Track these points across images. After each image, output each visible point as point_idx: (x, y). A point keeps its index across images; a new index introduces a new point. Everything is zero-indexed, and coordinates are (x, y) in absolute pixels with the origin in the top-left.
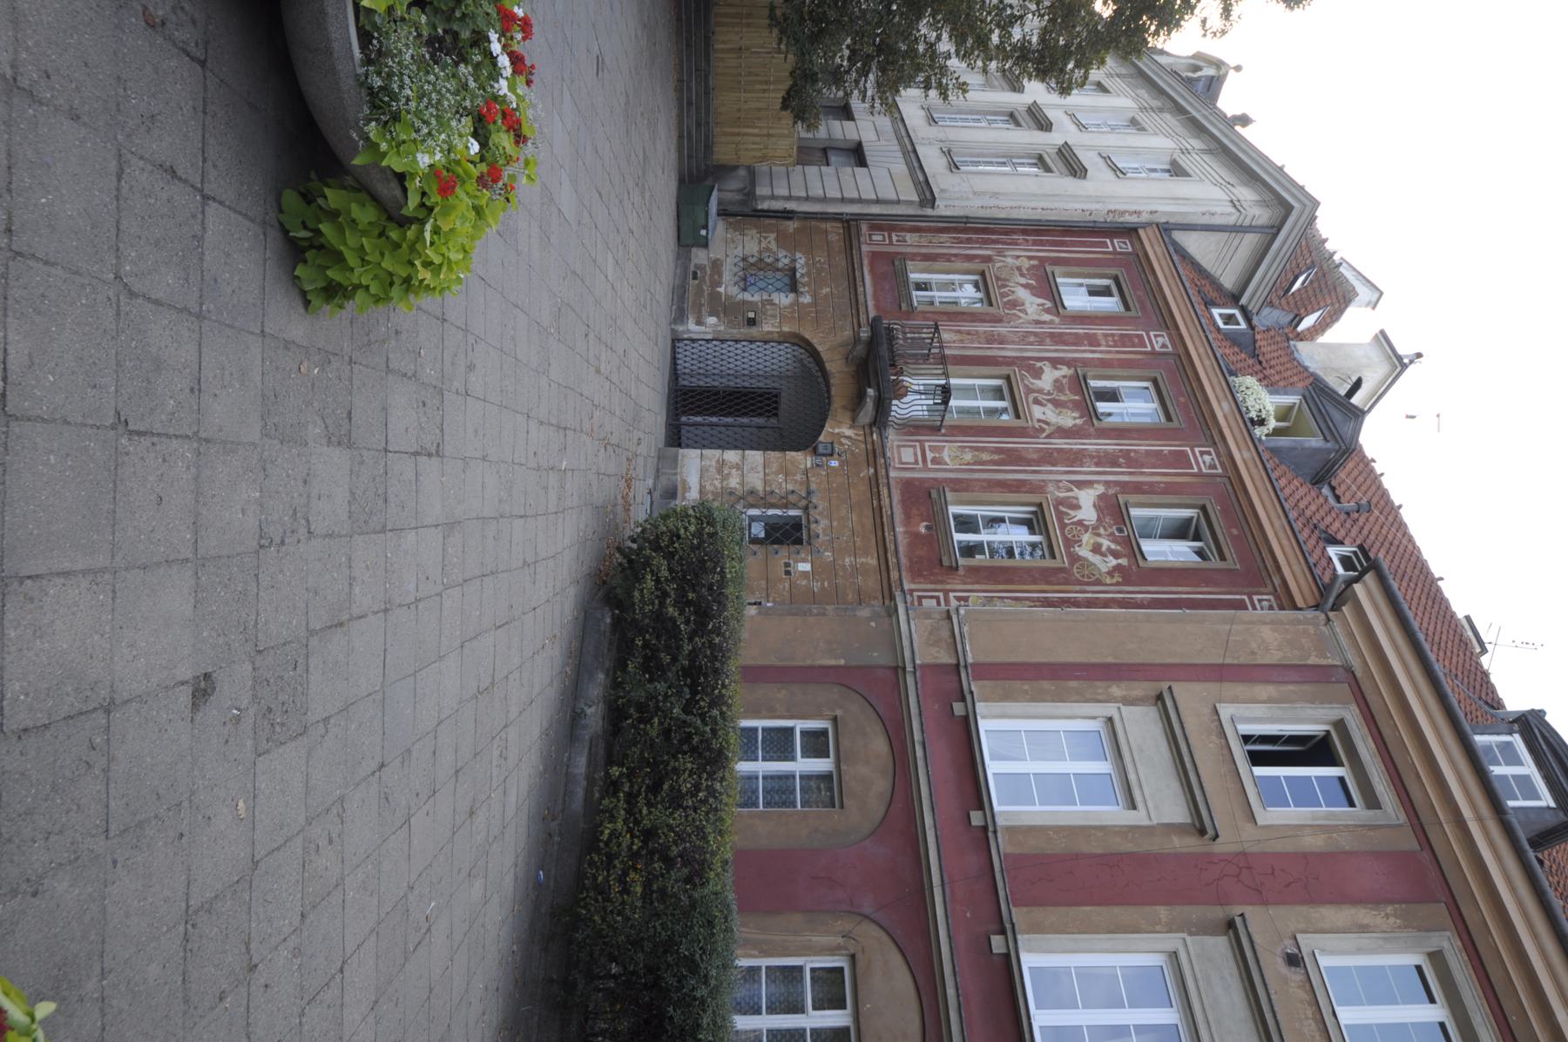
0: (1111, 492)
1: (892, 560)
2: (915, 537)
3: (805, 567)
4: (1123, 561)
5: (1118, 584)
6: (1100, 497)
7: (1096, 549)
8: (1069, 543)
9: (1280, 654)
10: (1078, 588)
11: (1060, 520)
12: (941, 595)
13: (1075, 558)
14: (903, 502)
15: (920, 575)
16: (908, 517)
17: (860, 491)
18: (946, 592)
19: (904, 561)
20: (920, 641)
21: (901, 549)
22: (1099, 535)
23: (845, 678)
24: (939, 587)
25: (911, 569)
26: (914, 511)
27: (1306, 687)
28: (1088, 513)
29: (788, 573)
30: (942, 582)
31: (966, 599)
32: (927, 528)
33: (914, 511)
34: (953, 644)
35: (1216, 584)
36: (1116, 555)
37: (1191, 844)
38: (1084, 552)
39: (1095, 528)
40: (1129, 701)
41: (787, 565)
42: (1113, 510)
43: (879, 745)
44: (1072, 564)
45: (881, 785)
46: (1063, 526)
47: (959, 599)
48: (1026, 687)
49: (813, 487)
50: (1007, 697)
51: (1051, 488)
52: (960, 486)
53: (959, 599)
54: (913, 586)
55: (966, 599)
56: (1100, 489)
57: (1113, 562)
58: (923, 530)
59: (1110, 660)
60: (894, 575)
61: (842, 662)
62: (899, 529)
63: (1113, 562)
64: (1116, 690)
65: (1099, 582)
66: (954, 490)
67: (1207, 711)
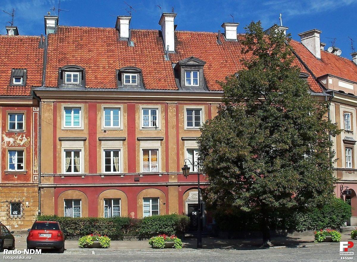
0: (5, 133)
1: (26, 185)
2: (18, 179)
3: (27, 203)
4: (24, 135)
5: (30, 138)
6: (6, 136)
7: (21, 140)
8: (19, 146)
9: (51, 113)
10: (31, 147)
11: (13, 146)
12: (34, 176)
13: (23, 145)
14: (9, 181)
15: (28, 179)
16: (13, 180)
17: (6, 190)
18: (33, 175)
19: (25, 182)
20: (49, 182)
21: (21, 183)
22: (17, 139)
23: (57, 197)
24: (32, 176)
25: (27, 181)
26: (11, 178)
27: (58, 111)
28: (11, 140)
29: (29, 207)
30: (30, 174)
31: (35, 171)
32: (16, 176)
33: (11, 178)
34: (50, 176)
35: (30, 117)
36: (22, 136)
37: (87, 141)
38: (22, 143)
39: (15, 139)
40: (61, 145)
41: (27, 207)
42: (9, 135)
43: (70, 192)
44: (25, 147)
45: (77, 192)
46: (14, 146)
47: (35, 172)
48: (58, 164)
49: (5, 201)
50: (60, 168)
51: (4, 147)
52: (4, 167)
53: (35, 172)
54: (32, 181)
55: (35, 171)
56: (4, 136)
57: (24, 138)
58: (16, 177)
59: (52, 147)
60: (30, 185)
61: (54, 198)
62: (16, 182)
63: (24, 138)
64: (58, 147)
65: (30, 142)
66: (5, 168)
67: (62, 131)
